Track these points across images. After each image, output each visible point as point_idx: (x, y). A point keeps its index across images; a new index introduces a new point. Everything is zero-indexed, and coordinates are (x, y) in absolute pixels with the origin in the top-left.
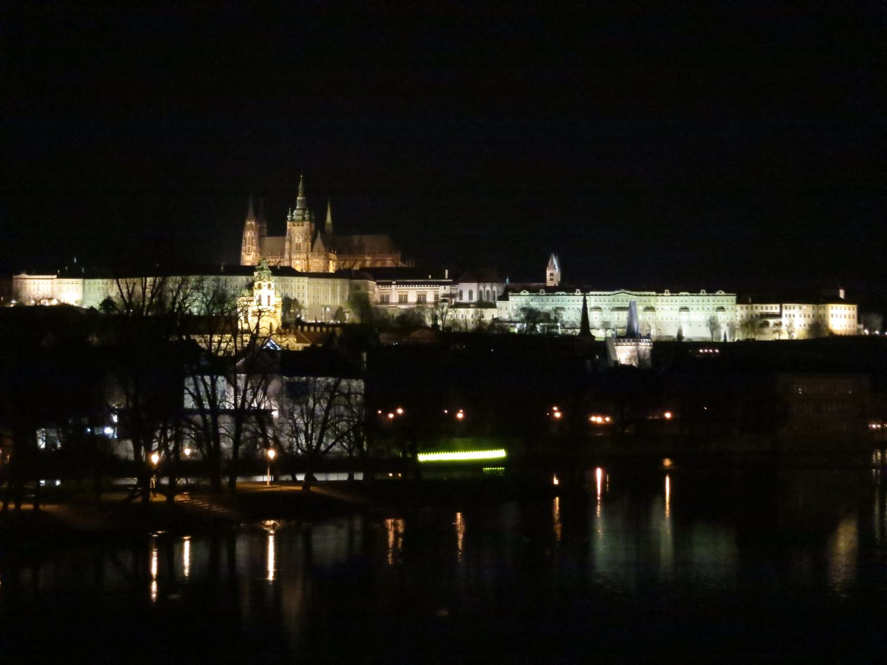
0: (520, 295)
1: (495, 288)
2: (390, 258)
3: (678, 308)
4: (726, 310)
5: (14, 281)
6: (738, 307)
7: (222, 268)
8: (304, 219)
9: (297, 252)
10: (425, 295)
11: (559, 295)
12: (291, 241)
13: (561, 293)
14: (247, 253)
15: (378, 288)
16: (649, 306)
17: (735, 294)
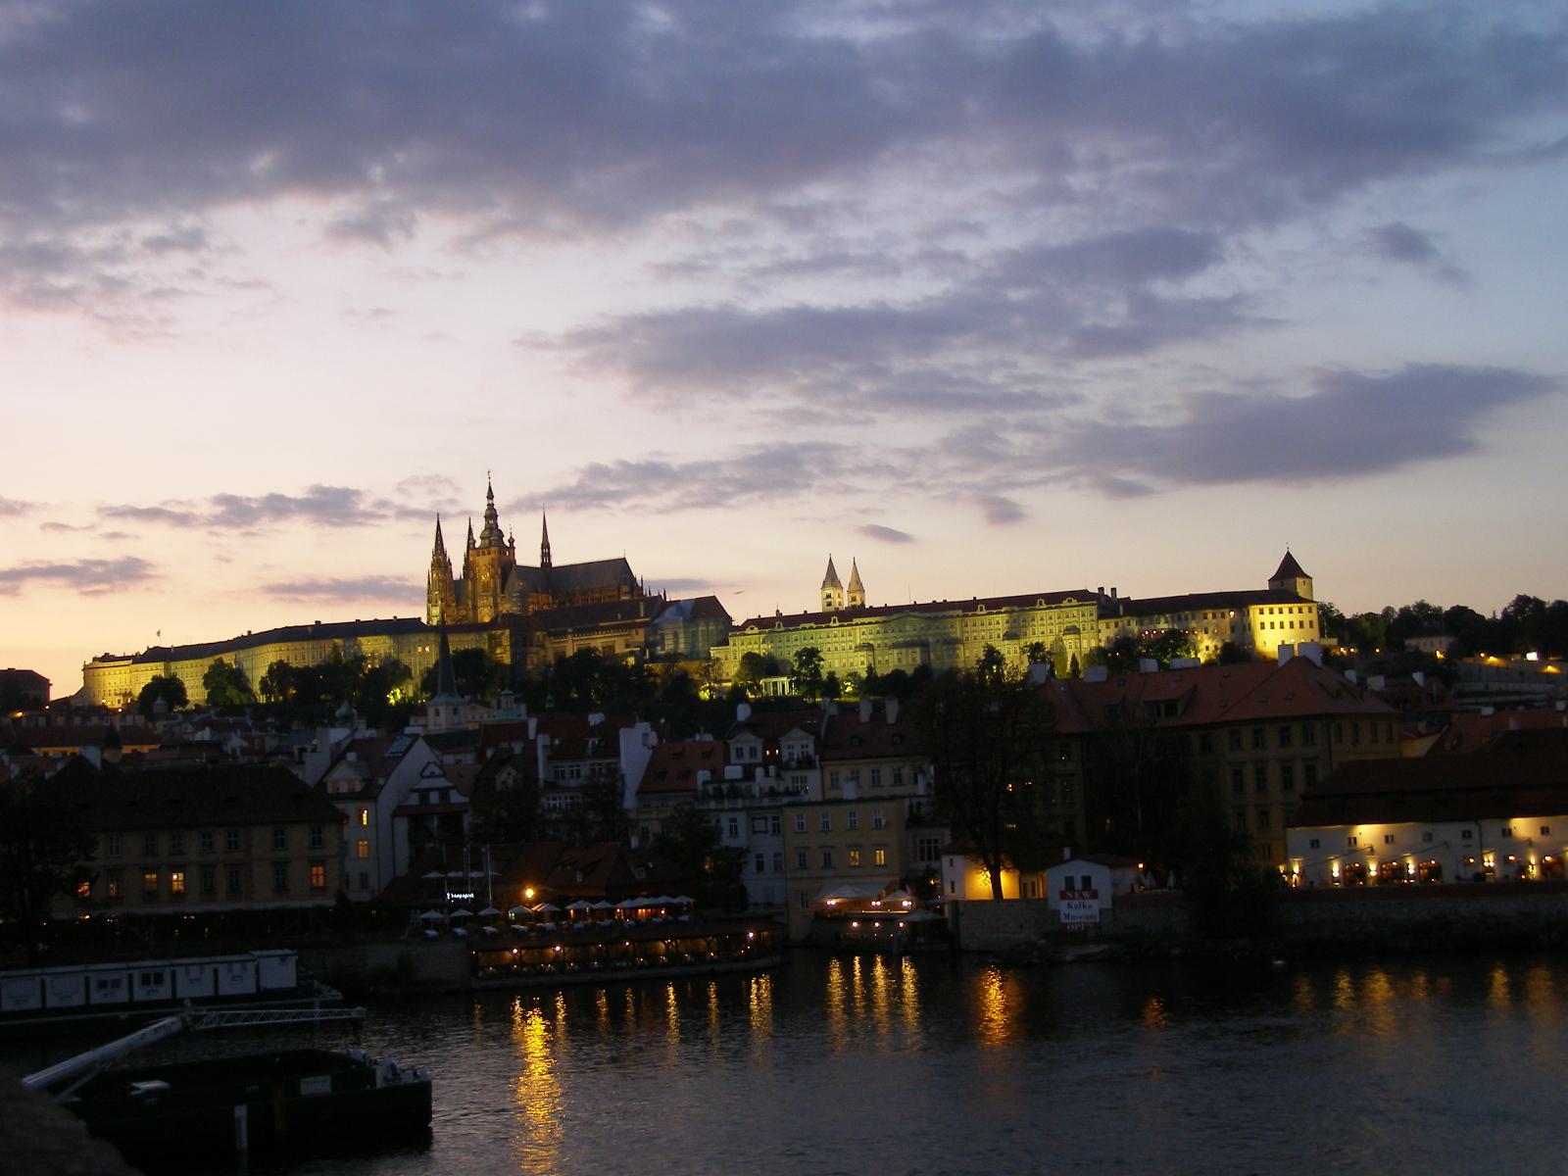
6: (1102, 624)
8: (490, 543)
11: (804, 628)
13: (807, 625)
14: (433, 603)
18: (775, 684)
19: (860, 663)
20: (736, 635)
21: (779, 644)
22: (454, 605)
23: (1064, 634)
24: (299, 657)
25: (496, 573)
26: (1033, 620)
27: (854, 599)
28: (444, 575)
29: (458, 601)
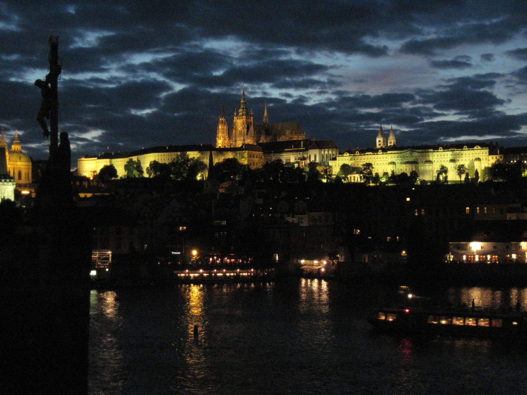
0: (343, 156)
1: (330, 152)
2: (296, 137)
3: (449, 160)
4: (482, 159)
5: (79, 162)
6: (490, 157)
7: (167, 148)
8: (243, 115)
9: (240, 136)
10: (290, 159)
11: (368, 155)
12: (236, 129)
14: (219, 138)
15: (264, 156)
16: (428, 159)
17: (488, 148)
18: (354, 177)
19: (389, 169)
20: (339, 156)
21: (357, 161)
22: (228, 139)
23: (474, 161)
24: (163, 160)
25: (245, 126)
26: (462, 154)
27: (391, 143)
28: (224, 127)
29: (230, 138)
